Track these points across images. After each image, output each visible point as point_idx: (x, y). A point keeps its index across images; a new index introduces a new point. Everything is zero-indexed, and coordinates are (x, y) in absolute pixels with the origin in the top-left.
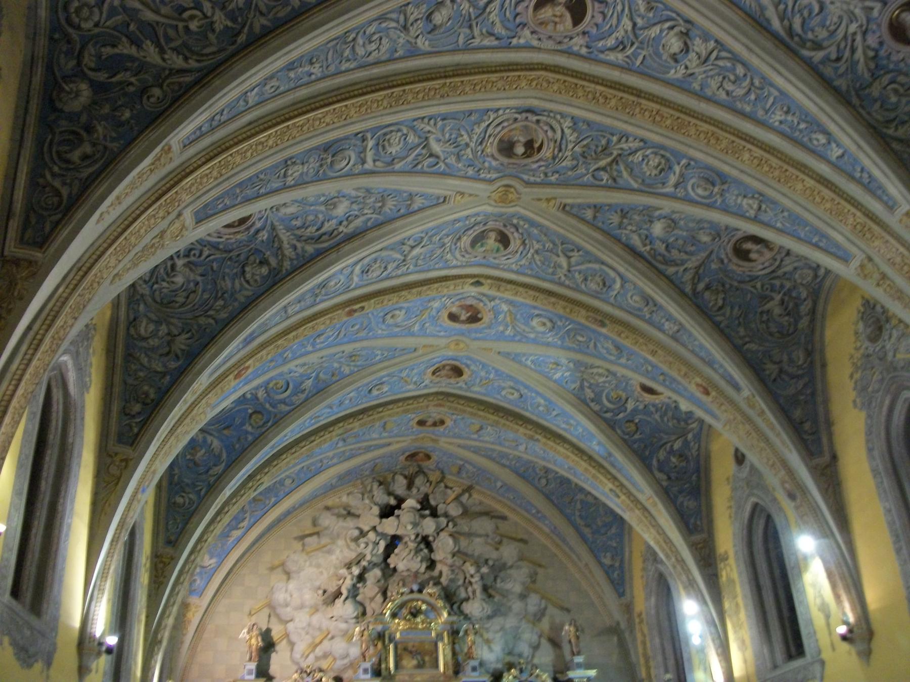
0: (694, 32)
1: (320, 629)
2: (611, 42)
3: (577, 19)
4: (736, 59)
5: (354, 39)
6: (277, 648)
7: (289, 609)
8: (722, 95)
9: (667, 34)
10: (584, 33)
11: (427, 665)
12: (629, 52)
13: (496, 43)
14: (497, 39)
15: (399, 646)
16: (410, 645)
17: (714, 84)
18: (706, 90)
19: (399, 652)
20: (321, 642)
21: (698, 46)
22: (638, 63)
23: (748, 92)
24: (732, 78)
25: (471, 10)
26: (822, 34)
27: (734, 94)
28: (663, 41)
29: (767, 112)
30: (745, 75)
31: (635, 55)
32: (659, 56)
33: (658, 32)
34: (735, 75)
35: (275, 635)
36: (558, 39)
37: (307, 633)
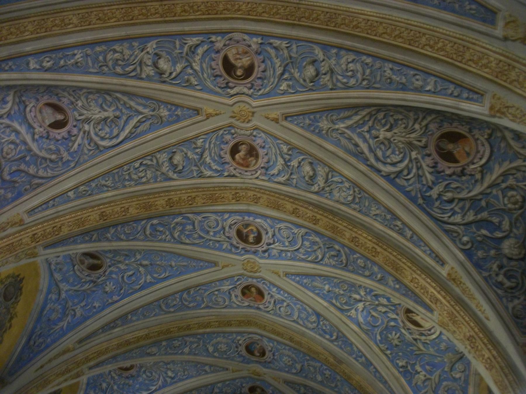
0: (157, 78)
2: (200, 51)
3: (226, 60)
4: (125, 75)
5: (363, 80)
8: (117, 47)
9: (171, 70)
10: (218, 52)
12: (186, 48)
13: (272, 41)
14: (271, 44)
17: (127, 52)
18: (128, 45)
21: (149, 71)
22: (177, 43)
23: (105, 58)
24: (120, 62)
25: (293, 71)
26: (91, 96)
27: (112, 53)
28: (171, 63)
29: (87, 55)
30: (114, 69)
31: (182, 47)
32: (168, 53)
33: (177, 68)
34: (120, 65)
36: (232, 42)
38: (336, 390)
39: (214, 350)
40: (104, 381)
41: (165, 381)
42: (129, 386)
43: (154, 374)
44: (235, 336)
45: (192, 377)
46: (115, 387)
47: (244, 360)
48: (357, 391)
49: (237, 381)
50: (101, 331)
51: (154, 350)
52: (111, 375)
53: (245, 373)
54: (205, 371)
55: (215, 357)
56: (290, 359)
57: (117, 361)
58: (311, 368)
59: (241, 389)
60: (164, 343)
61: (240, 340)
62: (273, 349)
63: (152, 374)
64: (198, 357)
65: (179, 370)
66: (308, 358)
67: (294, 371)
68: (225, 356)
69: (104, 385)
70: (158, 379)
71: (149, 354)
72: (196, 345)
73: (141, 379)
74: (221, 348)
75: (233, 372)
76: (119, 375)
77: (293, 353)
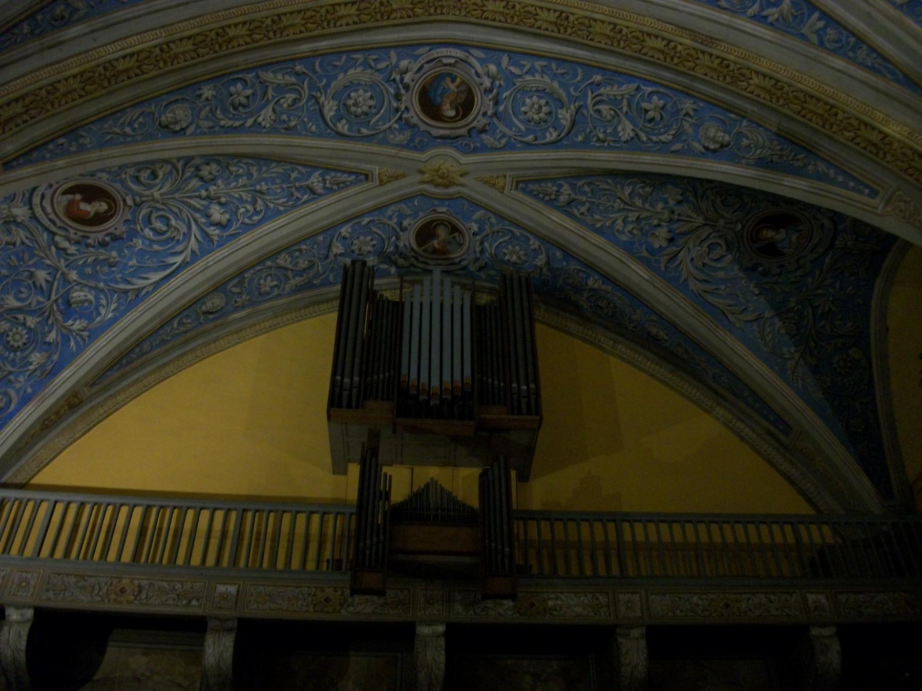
38: (677, 146)
39: (338, 111)
40: (39, 265)
41: (206, 235)
42: (111, 266)
43: (173, 222)
44: (394, 59)
45: (279, 213)
46: (73, 275)
47: (412, 139)
48: (745, 123)
49: (389, 212)
50: (26, 29)
51: (180, 113)
52: (56, 245)
53: (410, 184)
54: (313, 191)
55: (341, 135)
56: (543, 102)
57: (82, 149)
58: (604, 108)
59: (398, 238)
60: (208, 92)
61: (406, 72)
62: (497, 83)
63: (168, 225)
64: (296, 141)
65: (241, 200)
66: (598, 78)
67: (552, 135)
68: (365, 131)
69: (42, 275)
70: (187, 236)
71: (170, 131)
72: (291, 96)
73: (139, 243)
74: (356, 104)
75: (382, 183)
76: (78, 243)
77: (554, 77)
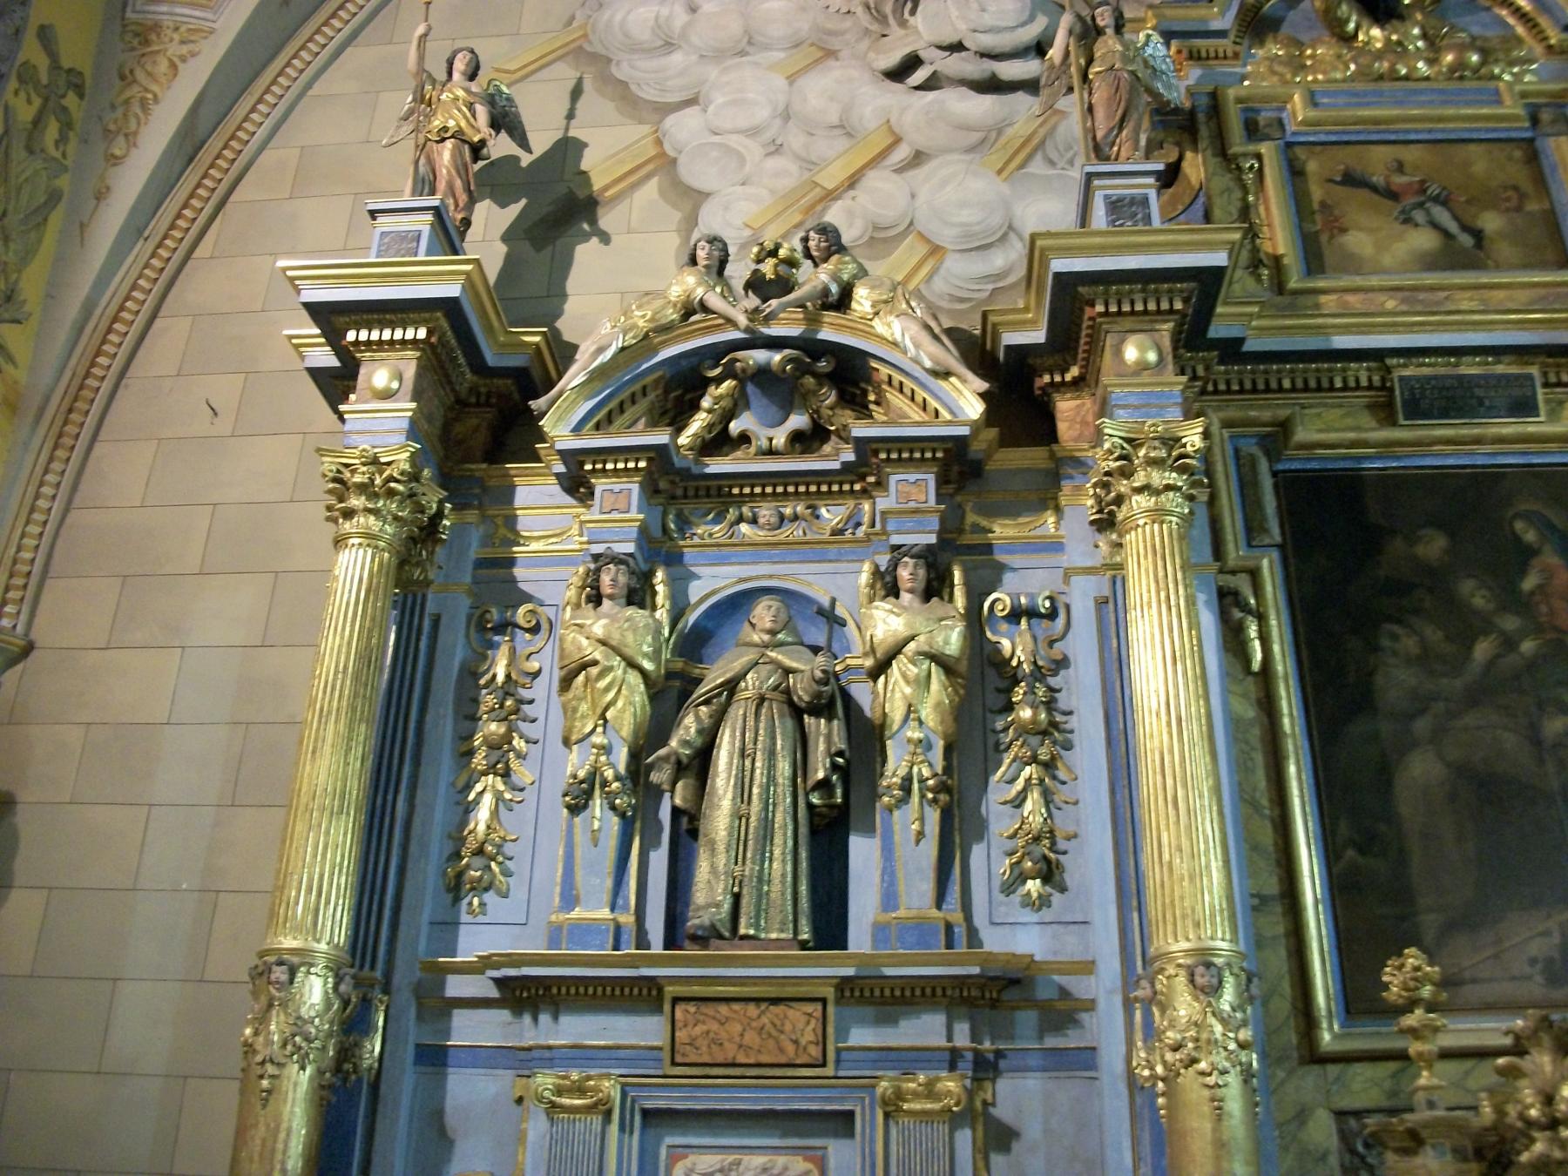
1: (844, 128)
6: (606, 221)
7: (677, 58)
11: (1504, 250)
15: (1312, 166)
16: (1376, 163)
19: (1317, 193)
20: (853, 182)
35: (599, 166)
37: (776, 149)
